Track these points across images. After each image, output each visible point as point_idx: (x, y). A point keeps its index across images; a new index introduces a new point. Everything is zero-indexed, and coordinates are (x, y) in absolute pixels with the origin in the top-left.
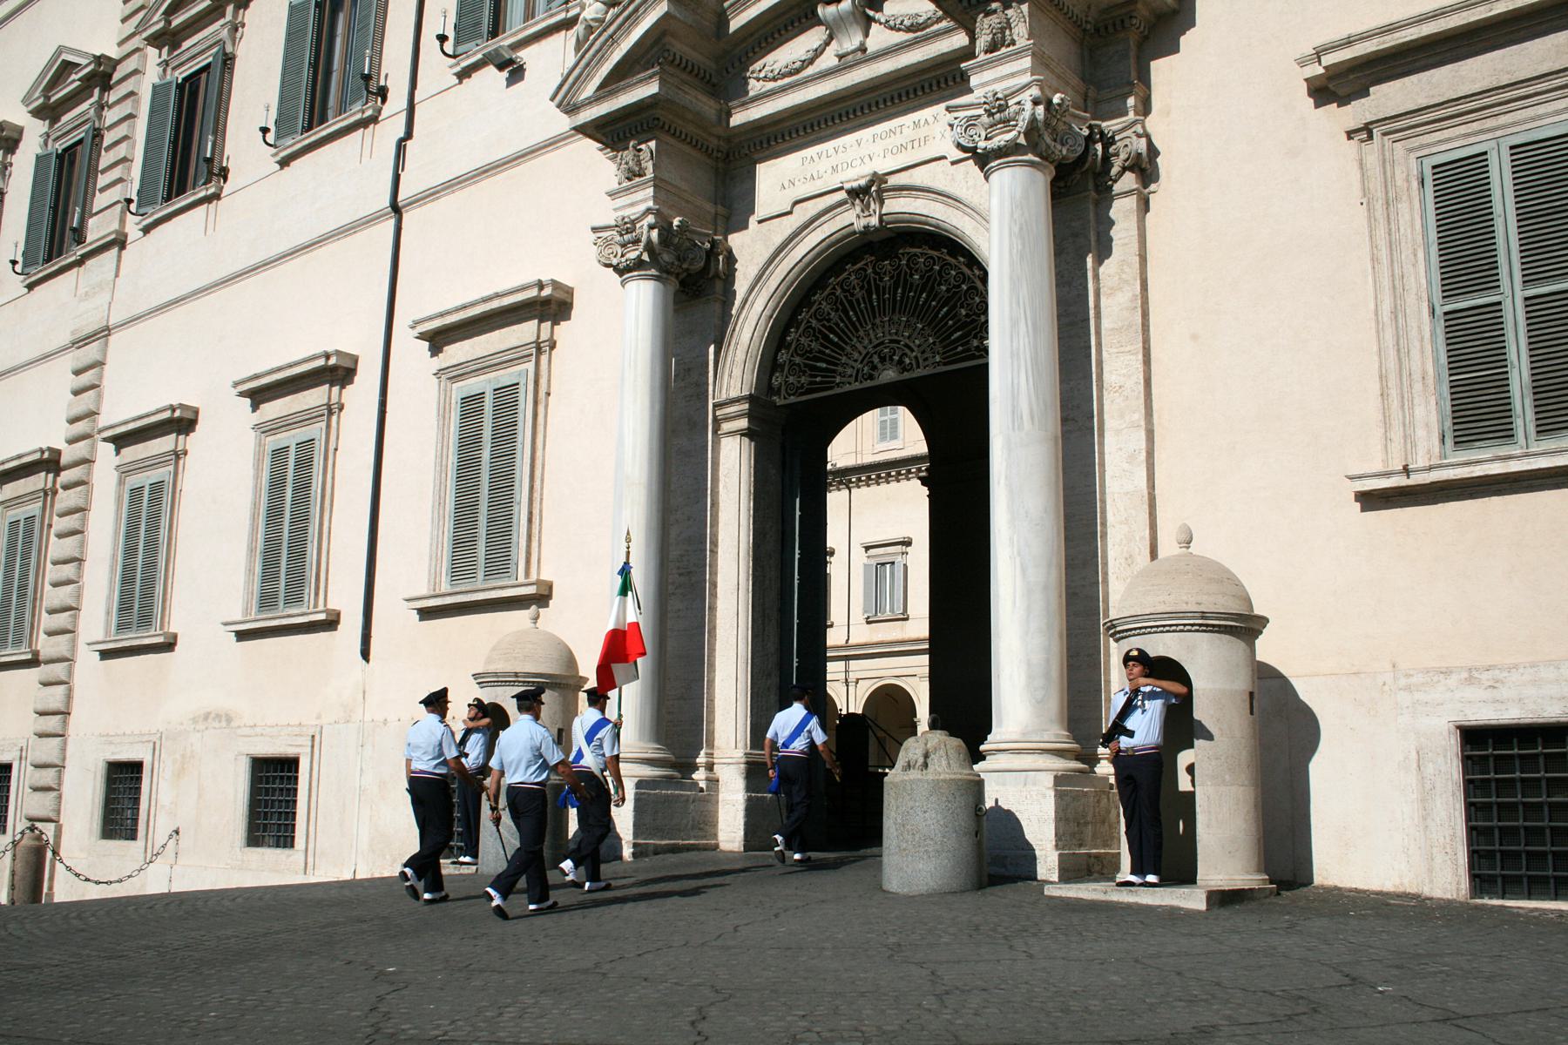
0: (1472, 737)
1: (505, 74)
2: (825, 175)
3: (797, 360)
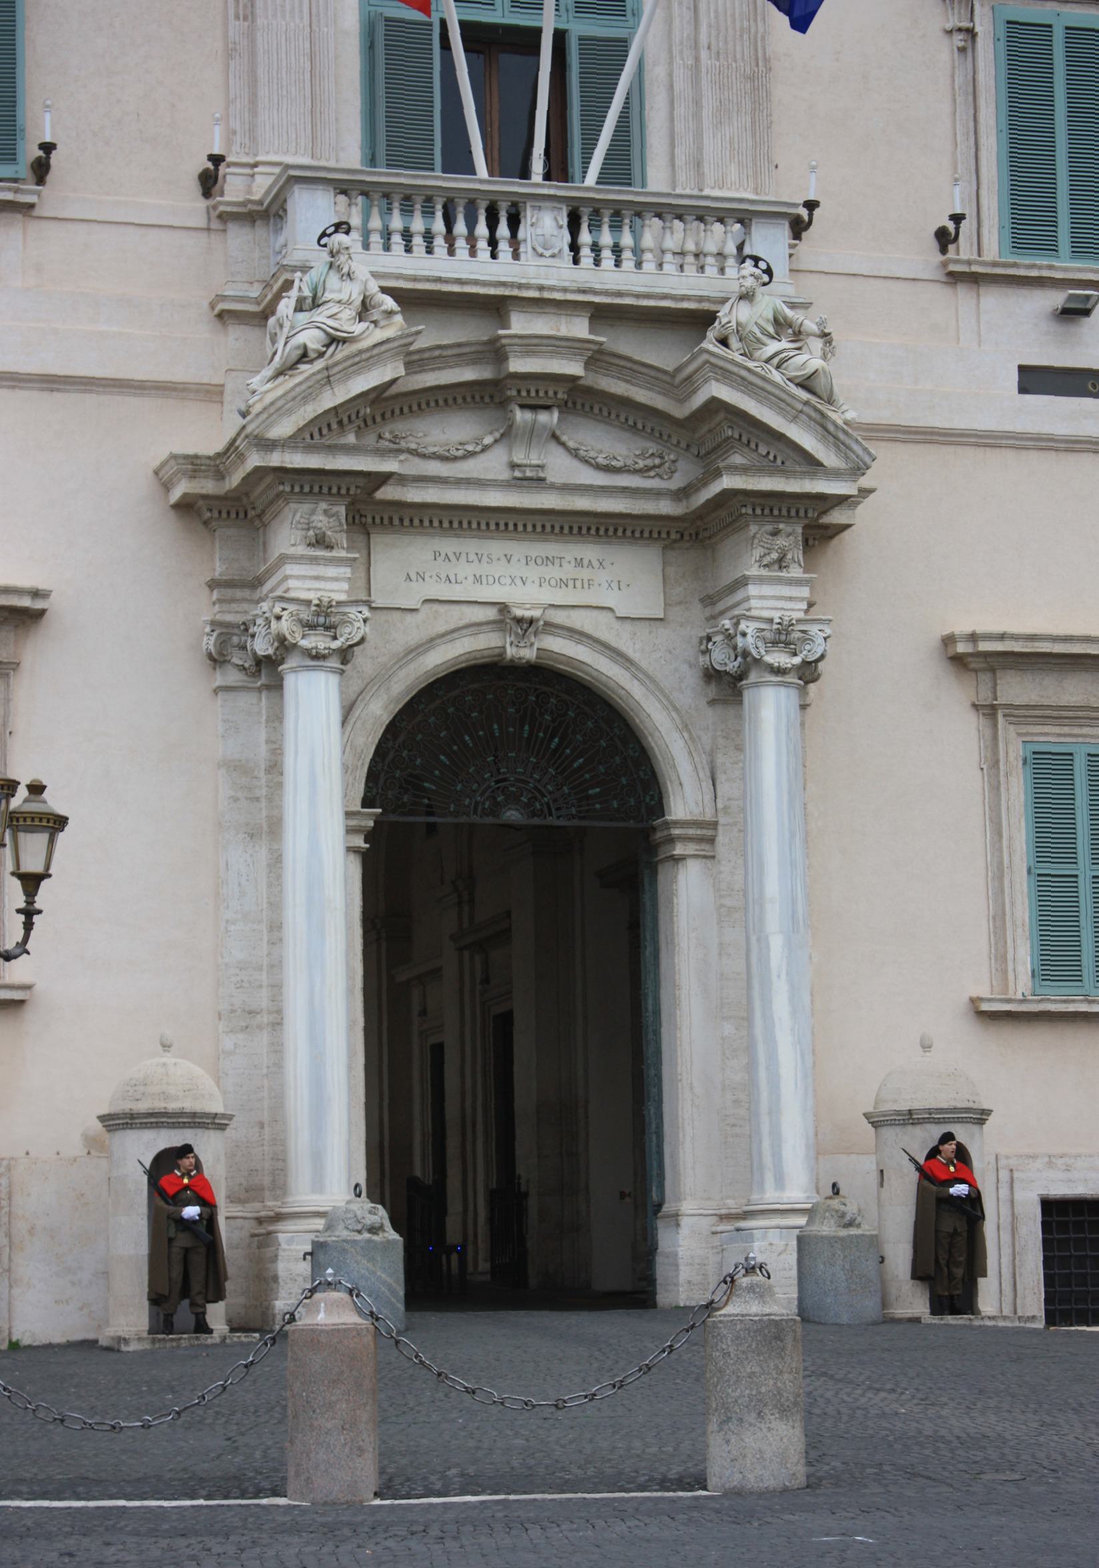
0: (1050, 1207)
2: (464, 581)
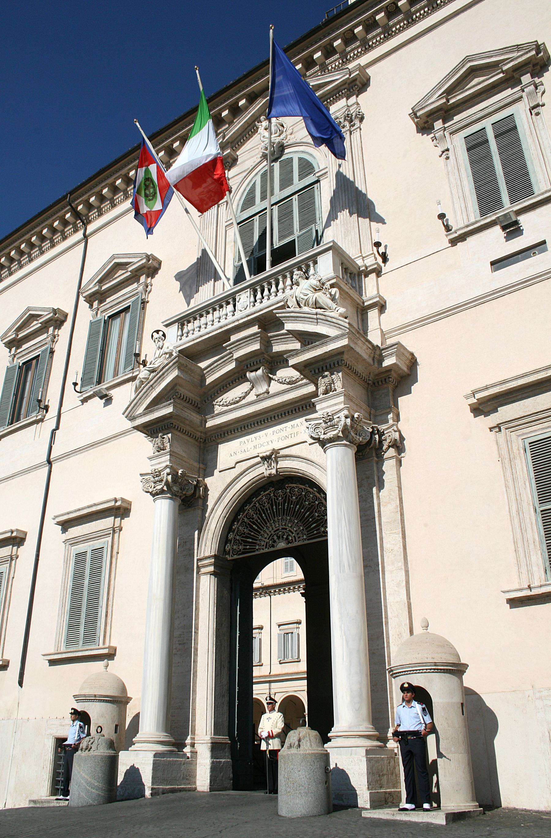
1: (103, 401)
3: (238, 538)
